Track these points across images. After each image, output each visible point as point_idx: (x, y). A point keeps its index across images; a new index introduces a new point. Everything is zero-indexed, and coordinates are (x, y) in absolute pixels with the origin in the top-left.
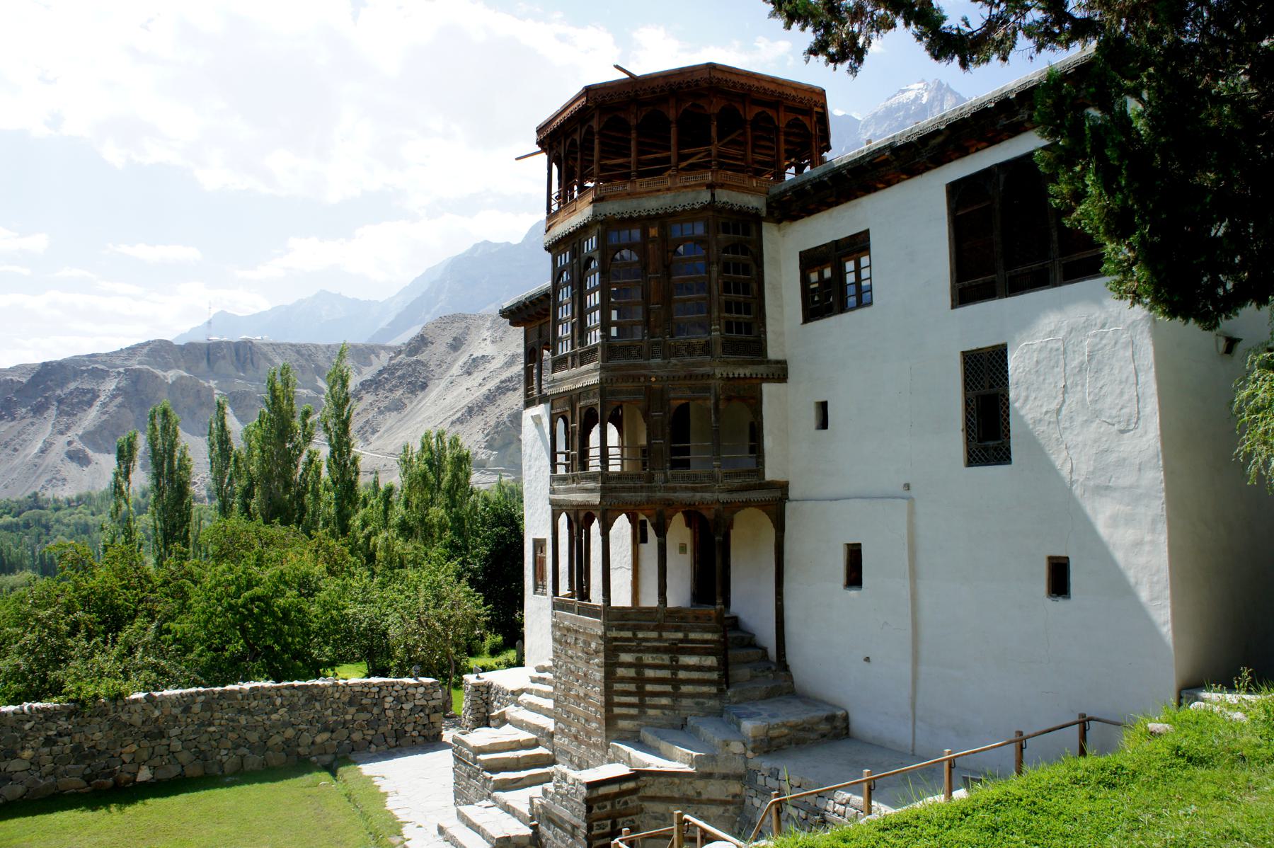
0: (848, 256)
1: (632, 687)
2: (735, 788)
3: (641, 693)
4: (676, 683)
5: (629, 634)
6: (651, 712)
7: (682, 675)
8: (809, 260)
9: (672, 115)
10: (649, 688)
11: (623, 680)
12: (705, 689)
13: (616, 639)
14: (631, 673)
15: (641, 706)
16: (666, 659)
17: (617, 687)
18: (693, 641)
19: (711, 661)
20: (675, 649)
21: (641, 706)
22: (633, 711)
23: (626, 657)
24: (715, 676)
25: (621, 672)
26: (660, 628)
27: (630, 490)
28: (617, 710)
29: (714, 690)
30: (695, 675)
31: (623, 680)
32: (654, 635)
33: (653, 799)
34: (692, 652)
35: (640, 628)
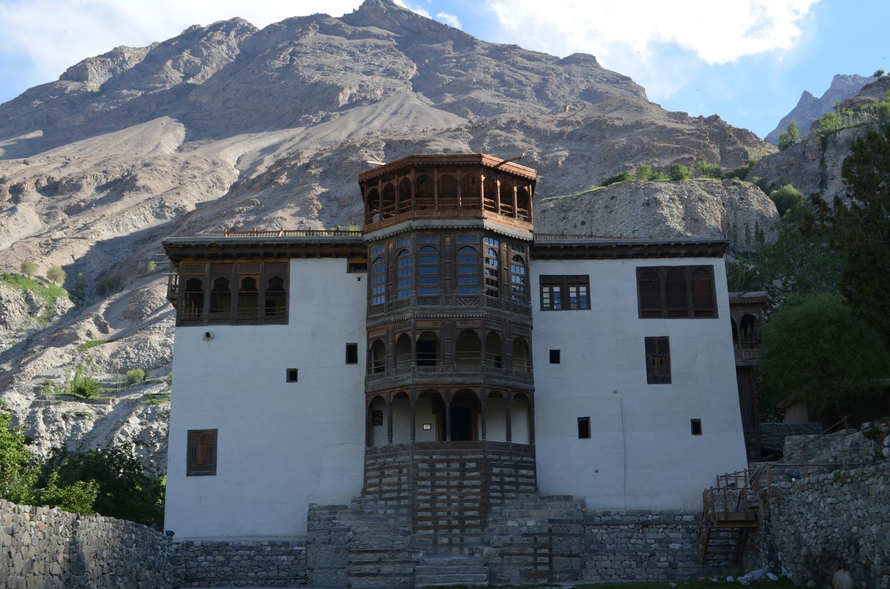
0: (573, 285)
1: (498, 488)
2: (579, 526)
3: (502, 491)
4: (517, 484)
5: (496, 457)
6: (507, 501)
7: (520, 480)
8: (546, 281)
10: (506, 487)
11: (494, 483)
12: (530, 488)
13: (491, 460)
14: (498, 479)
15: (502, 498)
17: (492, 487)
18: (524, 462)
19: (531, 473)
21: (502, 498)
22: (499, 501)
23: (496, 470)
24: (533, 481)
25: (494, 479)
26: (510, 454)
27: (498, 378)
28: (492, 501)
29: (532, 488)
30: (525, 480)
31: (494, 483)
32: (508, 458)
33: (555, 534)
34: (524, 468)
35: (500, 454)
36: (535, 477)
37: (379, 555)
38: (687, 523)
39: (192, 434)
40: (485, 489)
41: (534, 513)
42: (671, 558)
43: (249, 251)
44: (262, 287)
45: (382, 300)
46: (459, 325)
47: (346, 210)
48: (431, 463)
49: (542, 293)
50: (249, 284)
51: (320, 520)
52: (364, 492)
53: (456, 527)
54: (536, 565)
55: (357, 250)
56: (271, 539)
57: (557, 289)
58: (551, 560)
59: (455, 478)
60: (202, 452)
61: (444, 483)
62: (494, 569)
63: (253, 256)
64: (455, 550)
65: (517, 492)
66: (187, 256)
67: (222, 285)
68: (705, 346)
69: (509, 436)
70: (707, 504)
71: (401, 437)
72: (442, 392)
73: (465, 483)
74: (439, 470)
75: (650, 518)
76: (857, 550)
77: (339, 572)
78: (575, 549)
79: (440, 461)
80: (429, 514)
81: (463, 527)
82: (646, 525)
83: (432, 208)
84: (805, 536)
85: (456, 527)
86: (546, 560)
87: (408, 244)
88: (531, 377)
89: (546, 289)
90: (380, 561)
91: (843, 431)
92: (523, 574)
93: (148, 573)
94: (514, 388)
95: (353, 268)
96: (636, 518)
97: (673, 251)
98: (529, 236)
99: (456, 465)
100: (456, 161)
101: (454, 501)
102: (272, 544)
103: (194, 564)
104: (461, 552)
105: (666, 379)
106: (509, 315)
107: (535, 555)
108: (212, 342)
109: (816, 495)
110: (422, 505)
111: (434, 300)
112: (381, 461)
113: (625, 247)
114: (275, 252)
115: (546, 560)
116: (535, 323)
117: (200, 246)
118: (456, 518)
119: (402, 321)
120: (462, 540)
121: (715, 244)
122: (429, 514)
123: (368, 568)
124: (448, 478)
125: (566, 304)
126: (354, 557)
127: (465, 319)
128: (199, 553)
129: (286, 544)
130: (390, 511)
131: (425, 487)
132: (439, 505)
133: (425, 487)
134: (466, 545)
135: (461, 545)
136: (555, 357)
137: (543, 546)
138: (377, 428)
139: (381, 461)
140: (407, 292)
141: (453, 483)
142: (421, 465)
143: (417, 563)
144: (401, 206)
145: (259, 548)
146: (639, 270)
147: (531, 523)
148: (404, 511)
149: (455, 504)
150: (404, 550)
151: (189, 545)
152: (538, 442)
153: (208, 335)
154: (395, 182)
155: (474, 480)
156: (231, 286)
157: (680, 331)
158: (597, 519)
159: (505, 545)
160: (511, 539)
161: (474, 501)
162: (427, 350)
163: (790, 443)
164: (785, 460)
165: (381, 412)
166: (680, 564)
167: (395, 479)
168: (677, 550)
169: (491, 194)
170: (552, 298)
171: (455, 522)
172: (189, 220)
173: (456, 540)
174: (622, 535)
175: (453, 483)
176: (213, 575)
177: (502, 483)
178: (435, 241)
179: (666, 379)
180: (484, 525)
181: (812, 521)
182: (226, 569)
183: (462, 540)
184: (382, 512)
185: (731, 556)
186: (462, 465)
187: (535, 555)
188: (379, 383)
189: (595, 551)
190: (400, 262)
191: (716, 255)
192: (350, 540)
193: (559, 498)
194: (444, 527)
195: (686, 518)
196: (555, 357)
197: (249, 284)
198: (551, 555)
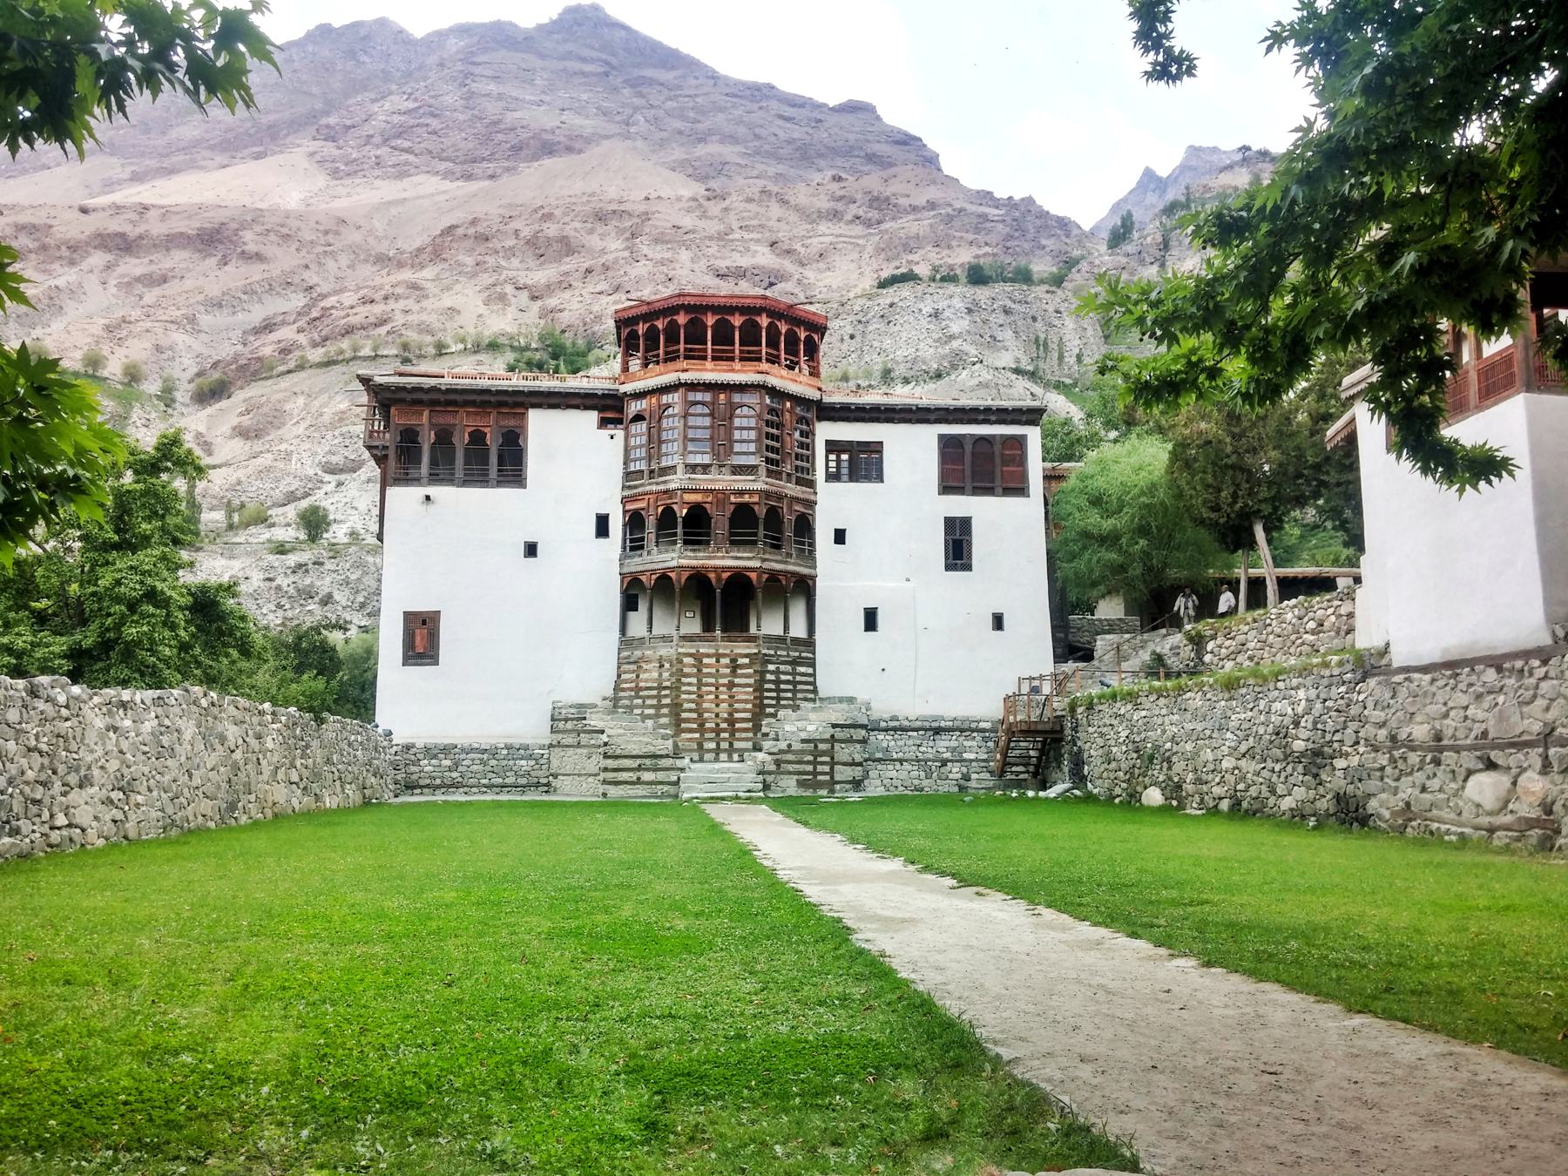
2: (863, 732)
3: (778, 690)
4: (795, 683)
7: (798, 678)
8: (833, 447)
9: (803, 336)
14: (772, 677)
15: (778, 699)
16: (789, 668)
19: (810, 670)
20: (795, 663)
21: (778, 699)
23: (771, 667)
25: (769, 677)
26: (788, 649)
30: (804, 679)
31: (770, 681)
34: (802, 664)
36: (814, 675)
37: (639, 761)
38: (983, 731)
39: (409, 616)
40: (759, 688)
41: (812, 716)
42: (964, 770)
43: (478, 398)
44: (493, 442)
45: (641, 466)
46: (733, 499)
47: (539, 303)
48: (698, 658)
49: (827, 461)
50: (477, 437)
51: (566, 720)
52: (617, 688)
53: (724, 730)
54: (815, 773)
55: (610, 402)
56: (509, 741)
57: (845, 457)
58: (832, 769)
59: (724, 676)
60: (422, 642)
61: (712, 680)
62: (770, 778)
63: (484, 404)
64: (723, 756)
65: (795, 691)
66: (402, 401)
67: (444, 439)
68: (1012, 529)
69: (786, 628)
70: (1008, 711)
71: (664, 625)
72: (712, 576)
73: (737, 681)
74: (708, 666)
75: (943, 724)
76: (1170, 768)
77: (591, 779)
78: (858, 758)
79: (708, 656)
80: (695, 715)
81: (733, 733)
82: (938, 731)
83: (705, 358)
84: (1114, 750)
85: (724, 730)
86: (827, 769)
87: (674, 398)
88: (814, 559)
89: (832, 457)
90: (639, 768)
91: (1164, 631)
92: (801, 784)
93: (373, 779)
94: (793, 574)
95: (604, 423)
96: (927, 724)
97: (981, 417)
98: (815, 395)
99: (725, 661)
100: (734, 302)
101: (723, 701)
102: (508, 747)
103: (416, 769)
104: (730, 760)
105: (968, 567)
106: (792, 489)
107: (815, 763)
108: (432, 508)
109: (1129, 706)
110: (686, 706)
111: (705, 468)
112: (638, 653)
113: (927, 410)
114: (510, 400)
115: (827, 769)
116: (819, 498)
117: (417, 389)
118: (725, 720)
119: (666, 492)
120: (731, 745)
121: (1031, 411)
122: (695, 715)
123: (625, 776)
124: (717, 675)
125: (854, 477)
126: (610, 763)
127: (741, 493)
128: (420, 756)
129: (526, 748)
130: (652, 711)
131: (689, 684)
132: (705, 705)
133: (689, 684)
134: (737, 750)
135: (731, 750)
136: (840, 536)
137: (823, 753)
138: (631, 614)
139: (638, 653)
140: (672, 456)
141: (722, 681)
142: (687, 660)
143: (682, 770)
144: (666, 353)
145: (493, 752)
146: (941, 437)
147: (811, 728)
148: (665, 711)
149: (724, 705)
150: (667, 756)
151: (408, 747)
152: (818, 636)
153: (428, 498)
154: (660, 324)
155: (746, 678)
156: (455, 440)
157: (983, 510)
158: (883, 724)
159: (781, 752)
160: (790, 746)
161: (746, 701)
162: (696, 526)
163: (1102, 644)
164: (1095, 662)
165: (636, 596)
166: (974, 776)
167: (655, 675)
168: (971, 761)
169: (774, 343)
170: (838, 467)
171: (724, 725)
172: (322, 304)
173: (725, 745)
174: (911, 742)
175: (722, 681)
176: (438, 781)
177: (778, 682)
178: (708, 397)
179: (968, 567)
180: (757, 728)
181: (1124, 734)
182: (455, 775)
183: (731, 745)
184: (638, 711)
185: (1031, 769)
186: (734, 660)
187: (815, 763)
188: (637, 563)
189: (879, 760)
190: (664, 421)
191: (1033, 423)
192: (606, 744)
193: (841, 700)
194: (712, 730)
195: (983, 725)
196: (840, 536)
197: (477, 437)
198: (833, 764)
